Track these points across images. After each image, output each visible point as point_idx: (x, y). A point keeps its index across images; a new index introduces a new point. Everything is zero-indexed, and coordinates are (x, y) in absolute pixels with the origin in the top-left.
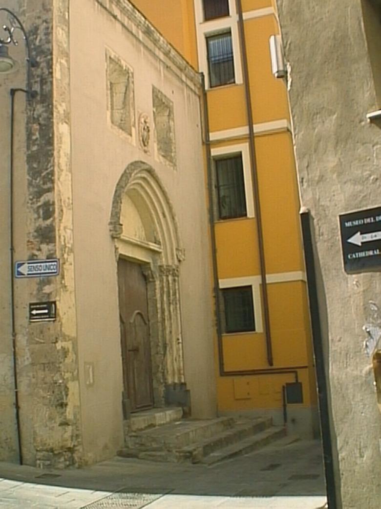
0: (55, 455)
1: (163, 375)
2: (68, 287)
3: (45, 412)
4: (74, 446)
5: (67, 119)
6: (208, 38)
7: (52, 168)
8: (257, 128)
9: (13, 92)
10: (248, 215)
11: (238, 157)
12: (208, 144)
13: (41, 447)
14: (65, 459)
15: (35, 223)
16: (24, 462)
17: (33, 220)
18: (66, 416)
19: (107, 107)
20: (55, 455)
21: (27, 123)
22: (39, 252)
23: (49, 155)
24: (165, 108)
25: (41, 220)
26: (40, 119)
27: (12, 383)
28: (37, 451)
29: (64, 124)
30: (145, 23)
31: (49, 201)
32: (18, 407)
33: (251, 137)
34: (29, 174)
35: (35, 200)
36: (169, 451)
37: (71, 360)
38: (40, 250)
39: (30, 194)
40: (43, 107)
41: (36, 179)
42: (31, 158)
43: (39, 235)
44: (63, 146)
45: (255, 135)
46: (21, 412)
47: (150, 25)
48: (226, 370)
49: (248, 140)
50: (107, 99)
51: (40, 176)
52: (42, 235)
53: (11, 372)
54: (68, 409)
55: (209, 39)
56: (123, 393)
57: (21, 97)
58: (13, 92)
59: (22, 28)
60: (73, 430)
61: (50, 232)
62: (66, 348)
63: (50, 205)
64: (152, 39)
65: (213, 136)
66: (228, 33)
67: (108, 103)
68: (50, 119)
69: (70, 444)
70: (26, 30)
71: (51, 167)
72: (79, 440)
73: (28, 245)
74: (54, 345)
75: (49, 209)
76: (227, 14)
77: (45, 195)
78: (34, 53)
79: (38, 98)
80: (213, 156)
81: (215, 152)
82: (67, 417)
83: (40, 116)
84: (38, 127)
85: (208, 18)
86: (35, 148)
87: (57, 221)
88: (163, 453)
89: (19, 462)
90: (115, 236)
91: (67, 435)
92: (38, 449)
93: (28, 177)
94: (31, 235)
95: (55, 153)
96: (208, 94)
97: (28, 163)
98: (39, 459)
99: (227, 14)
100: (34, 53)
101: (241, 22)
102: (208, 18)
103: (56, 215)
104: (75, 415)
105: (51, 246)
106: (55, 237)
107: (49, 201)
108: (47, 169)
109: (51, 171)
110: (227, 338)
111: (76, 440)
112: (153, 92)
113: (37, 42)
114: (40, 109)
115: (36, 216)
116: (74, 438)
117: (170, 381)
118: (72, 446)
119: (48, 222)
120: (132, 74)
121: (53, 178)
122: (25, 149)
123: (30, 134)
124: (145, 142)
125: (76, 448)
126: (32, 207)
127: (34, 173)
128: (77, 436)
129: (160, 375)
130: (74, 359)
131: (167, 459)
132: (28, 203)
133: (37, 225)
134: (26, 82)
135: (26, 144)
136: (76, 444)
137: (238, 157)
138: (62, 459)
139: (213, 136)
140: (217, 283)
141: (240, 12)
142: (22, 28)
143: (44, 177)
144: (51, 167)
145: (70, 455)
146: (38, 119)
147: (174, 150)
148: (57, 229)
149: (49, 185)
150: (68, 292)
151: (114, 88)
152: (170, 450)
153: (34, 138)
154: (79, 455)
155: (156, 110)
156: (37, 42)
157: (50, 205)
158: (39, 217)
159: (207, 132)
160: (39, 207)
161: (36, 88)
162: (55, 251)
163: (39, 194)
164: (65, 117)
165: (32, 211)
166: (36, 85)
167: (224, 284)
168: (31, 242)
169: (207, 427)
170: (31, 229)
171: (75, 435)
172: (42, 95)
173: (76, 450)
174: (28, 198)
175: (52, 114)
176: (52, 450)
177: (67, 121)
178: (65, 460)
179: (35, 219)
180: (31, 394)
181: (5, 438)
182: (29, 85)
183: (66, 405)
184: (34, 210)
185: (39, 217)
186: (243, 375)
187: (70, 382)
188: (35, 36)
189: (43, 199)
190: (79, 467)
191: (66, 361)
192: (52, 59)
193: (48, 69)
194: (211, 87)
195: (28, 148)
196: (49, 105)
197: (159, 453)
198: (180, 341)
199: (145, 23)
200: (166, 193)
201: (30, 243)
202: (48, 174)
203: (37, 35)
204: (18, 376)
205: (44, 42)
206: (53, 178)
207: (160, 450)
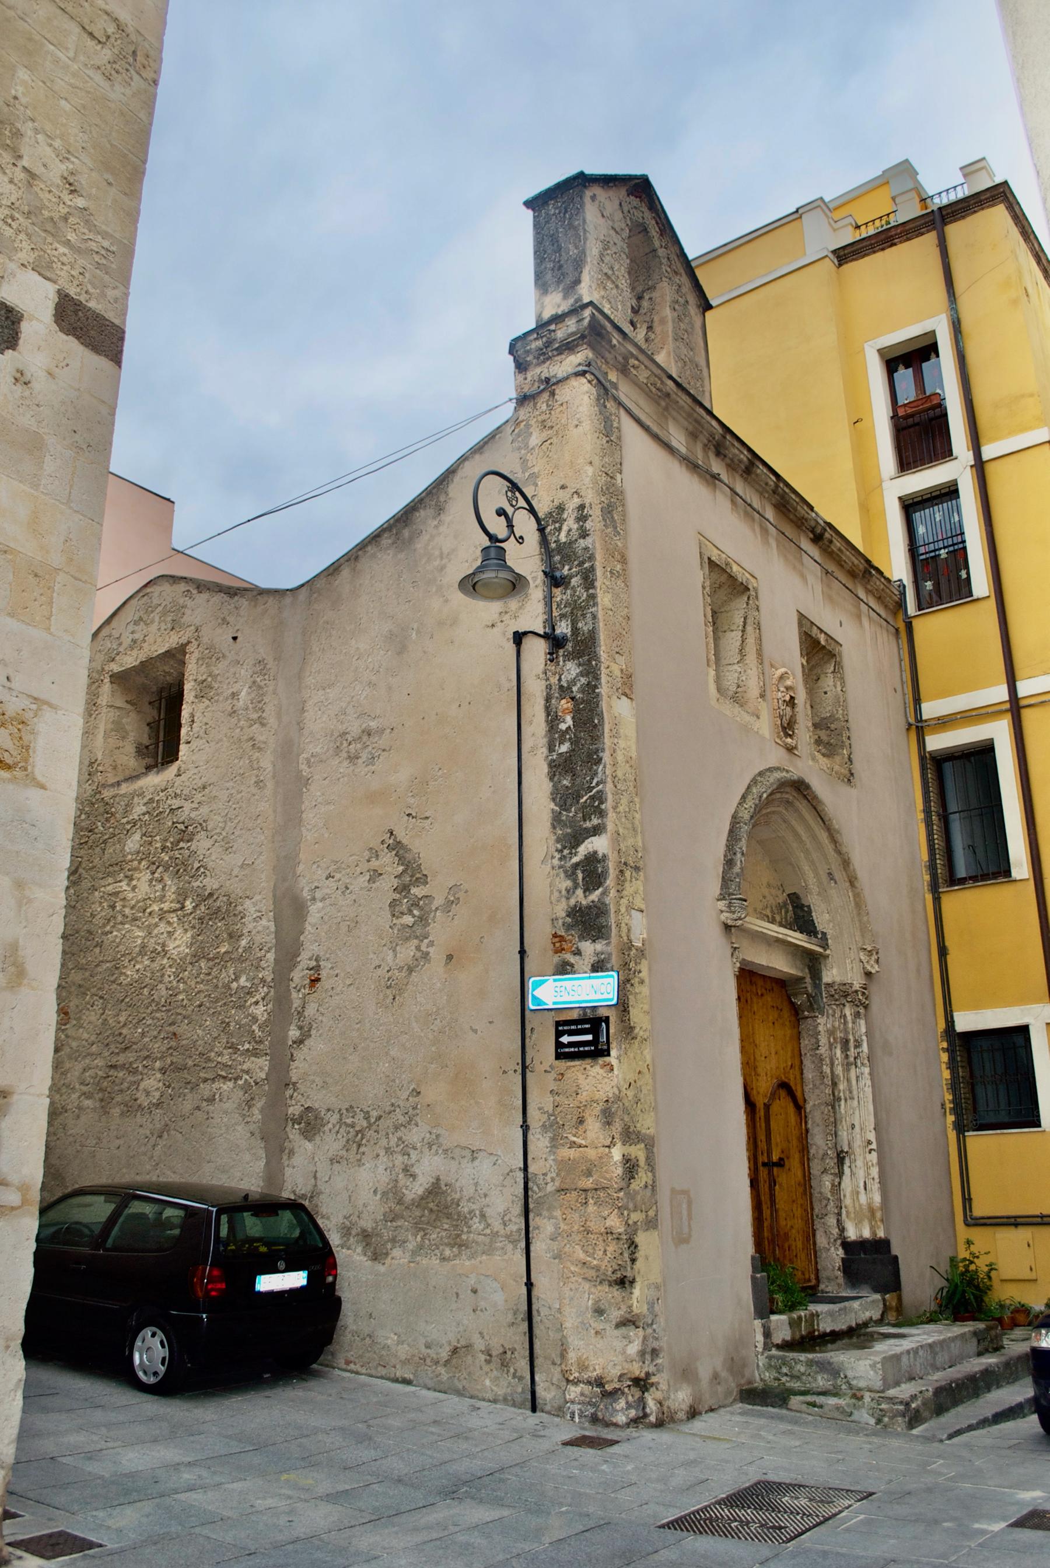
0: (606, 1394)
1: (839, 1222)
2: (636, 1031)
3: (588, 1295)
4: (648, 1374)
5: (627, 689)
6: (911, 506)
7: (600, 787)
8: (1024, 688)
9: (519, 638)
10: (1016, 873)
11: (985, 752)
12: (919, 728)
13: (577, 1375)
14: (627, 1403)
15: (568, 899)
16: (539, 1407)
17: (564, 892)
18: (630, 1307)
19: (708, 661)
20: (606, 1394)
21: (548, 699)
22: (577, 957)
23: (594, 759)
24: (826, 658)
25: (580, 892)
26: (575, 689)
27: (519, 1230)
28: (568, 1381)
29: (624, 698)
30: (777, 486)
31: (595, 852)
32: (529, 1285)
33: (1015, 708)
34: (554, 800)
35: (566, 852)
36: (854, 1396)
37: (642, 1184)
38: (578, 953)
39: (558, 841)
40: (580, 665)
41: (568, 810)
42: (559, 767)
43: (577, 922)
44: (622, 744)
45: (1023, 703)
46: (535, 1293)
47: (787, 490)
48: (978, 1211)
49: (1009, 716)
50: (707, 644)
51: (578, 802)
52: (584, 923)
53: (518, 1209)
54: (637, 1292)
55: (911, 510)
56: (753, 1258)
57: (536, 650)
58: (519, 638)
59: (532, 511)
60: (645, 1338)
61: (598, 916)
62: (633, 1157)
63: (599, 861)
64: (792, 517)
65: (930, 709)
66: (949, 492)
67: (708, 653)
68: (591, 688)
69: (637, 1370)
70: (541, 515)
71: (597, 784)
72: (659, 1361)
73: (554, 944)
74: (607, 1150)
75: (597, 870)
76: (945, 452)
77: (586, 842)
78: (557, 558)
79: (569, 646)
80: (929, 752)
81: (936, 742)
82: (634, 1308)
83: (573, 682)
84: (570, 705)
85: (906, 463)
86: (564, 748)
87: (613, 893)
88: (841, 1402)
89: (529, 1404)
90: (730, 922)
91: (633, 1349)
92: (571, 1378)
93: (552, 806)
94: (560, 922)
95: (606, 756)
96: (917, 624)
97: (551, 779)
98: (573, 1402)
99: (945, 452)
100: (557, 558)
101: (980, 467)
102: (906, 463)
103: (610, 881)
104: (651, 1305)
105: (599, 946)
106: (608, 927)
107: (595, 852)
108: (590, 789)
109: (598, 792)
110: (979, 1142)
111: (652, 1360)
112: (800, 625)
113: (563, 538)
114: (571, 669)
115: (569, 883)
116: (648, 1357)
117: (852, 1234)
118: (643, 1375)
119: (595, 896)
120: (756, 590)
121: (603, 807)
122: (545, 750)
123: (552, 719)
124: (787, 728)
125: (653, 1379)
126: (560, 867)
127: (564, 799)
128: (655, 1353)
129: (832, 1221)
130: (650, 1182)
131: (851, 1414)
132: (553, 857)
133: (572, 902)
134: (542, 618)
135: (545, 741)
136: (652, 1369)
137: (985, 752)
138: (622, 1404)
139: (930, 709)
140: (950, 1022)
141: (976, 443)
142: (532, 511)
143: (584, 806)
144: (597, 784)
145: (638, 1394)
146: (569, 688)
147: (847, 742)
148: (612, 911)
149: (595, 821)
150: (636, 1042)
151: (718, 622)
152: (858, 1394)
153: (563, 727)
154: (659, 1395)
155: (807, 662)
156: (563, 538)
157: (599, 861)
158: (576, 886)
159: (917, 701)
160: (577, 865)
161: (563, 628)
162: (610, 954)
163: (575, 839)
164: (624, 683)
165: (562, 875)
166: (563, 624)
167: (966, 1021)
168: (561, 936)
169: (942, 1343)
170: (561, 910)
171: (649, 1350)
172: (577, 643)
173: (652, 1384)
174: (554, 849)
175: (597, 678)
176: (599, 1382)
177: (627, 691)
178: (629, 1406)
179: (568, 891)
180: (558, 1256)
181: (501, 1350)
182: (550, 622)
183: (632, 1282)
184: (566, 872)
185: (576, 886)
186: (1016, 1225)
187: (639, 1233)
188: (557, 525)
189: (583, 850)
190: (659, 1424)
191: (632, 1186)
192: (592, 569)
193: (587, 589)
194: (920, 608)
195: (551, 749)
196: (589, 661)
197: (832, 1401)
198: (874, 1146)
199: (777, 486)
200: (820, 802)
201: (557, 940)
202: (592, 798)
203: (562, 521)
204: (531, 1216)
205: (575, 534)
206: (603, 807)
207: (836, 1393)
